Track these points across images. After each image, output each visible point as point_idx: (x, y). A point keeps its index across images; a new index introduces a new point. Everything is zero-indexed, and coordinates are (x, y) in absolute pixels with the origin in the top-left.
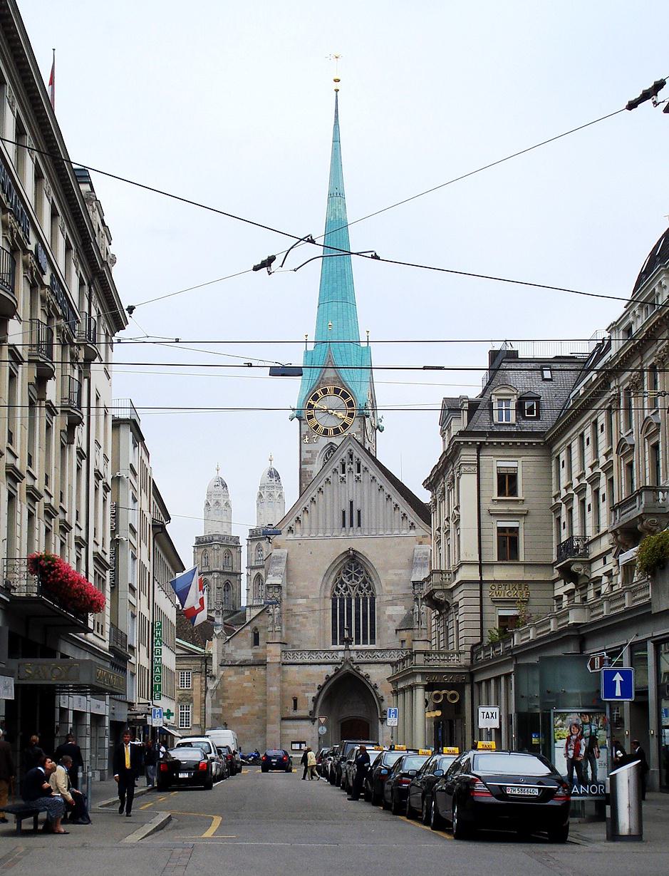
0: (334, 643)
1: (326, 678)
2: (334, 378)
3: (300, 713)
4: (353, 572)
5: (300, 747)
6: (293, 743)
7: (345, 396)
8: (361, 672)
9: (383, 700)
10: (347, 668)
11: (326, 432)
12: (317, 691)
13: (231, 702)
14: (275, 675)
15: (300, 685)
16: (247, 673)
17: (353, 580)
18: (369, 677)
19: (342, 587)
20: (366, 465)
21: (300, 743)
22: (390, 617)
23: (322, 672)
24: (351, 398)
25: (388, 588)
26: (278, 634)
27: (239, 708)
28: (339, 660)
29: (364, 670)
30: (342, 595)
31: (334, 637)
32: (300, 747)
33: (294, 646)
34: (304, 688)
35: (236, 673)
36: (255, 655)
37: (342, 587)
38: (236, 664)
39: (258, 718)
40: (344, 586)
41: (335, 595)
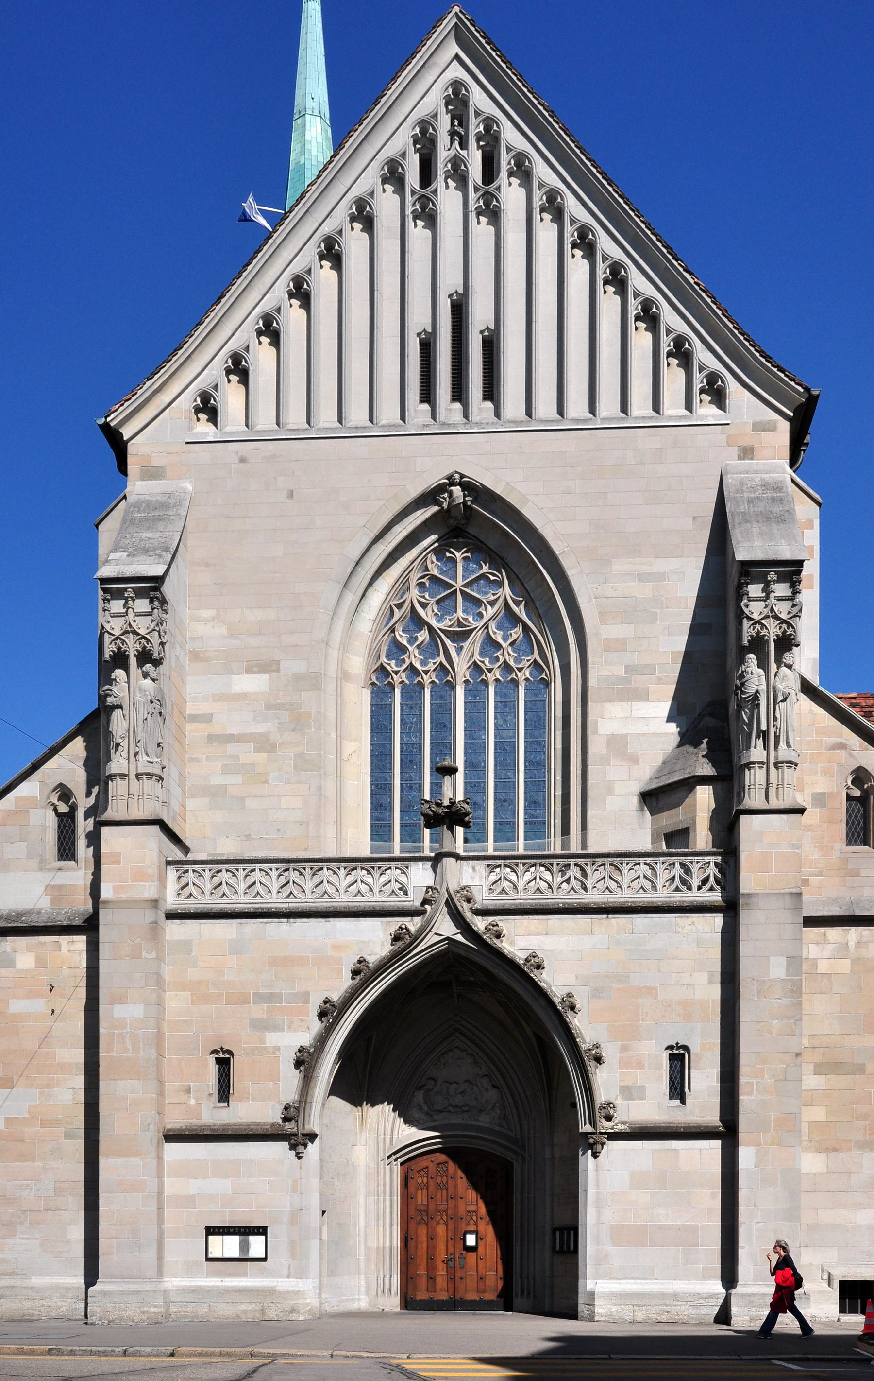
1: (355, 973)
4: (459, 583)
5: (244, 1247)
6: (211, 1231)
8: (506, 946)
12: (317, 1026)
14: (136, 955)
15: (243, 999)
17: (460, 613)
18: (539, 967)
19: (412, 640)
21: (245, 1231)
23: (337, 947)
28: (414, 900)
32: (244, 1247)
34: (259, 1011)
36: (56, 892)
41: (382, 671)
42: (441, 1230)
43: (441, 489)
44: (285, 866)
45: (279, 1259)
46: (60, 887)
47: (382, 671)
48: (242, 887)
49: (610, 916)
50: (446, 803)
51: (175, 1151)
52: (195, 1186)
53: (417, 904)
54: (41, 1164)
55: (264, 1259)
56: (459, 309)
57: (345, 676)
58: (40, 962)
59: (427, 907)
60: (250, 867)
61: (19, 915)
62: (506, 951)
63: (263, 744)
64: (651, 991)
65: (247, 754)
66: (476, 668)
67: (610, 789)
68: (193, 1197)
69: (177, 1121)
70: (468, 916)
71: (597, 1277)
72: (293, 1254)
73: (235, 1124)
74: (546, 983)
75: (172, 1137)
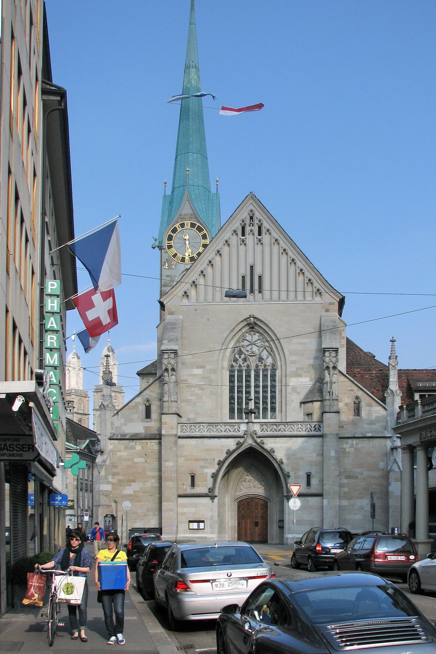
0: (232, 416)
2: (191, 214)
3: (198, 490)
5: (198, 526)
6: (190, 522)
7: (200, 229)
8: (265, 446)
9: (289, 476)
10: (250, 442)
11: (183, 260)
12: (217, 467)
13: (121, 477)
14: (171, 449)
15: (198, 460)
16: (138, 448)
18: (274, 452)
19: (240, 357)
20: (268, 227)
21: (199, 522)
22: (294, 389)
23: (222, 446)
24: (205, 232)
25: (293, 358)
26: (174, 404)
27: (130, 485)
28: (241, 433)
29: (269, 444)
30: (240, 366)
31: (232, 410)
32: (198, 526)
33: (189, 419)
34: (202, 463)
35: (126, 448)
36: (146, 428)
37: (240, 357)
38: (127, 437)
39: (150, 496)
40: (243, 356)
41: (232, 366)
42: (248, 521)
43: (248, 318)
44: (209, 424)
45: (208, 529)
46: (147, 427)
47: (232, 366)
48: (197, 430)
49: (292, 438)
50: (250, 409)
51: (181, 500)
52: (186, 510)
53: (242, 435)
54: (143, 503)
55: (204, 529)
56: (252, 267)
57: (223, 368)
58: (143, 448)
59: (245, 436)
60: (200, 425)
61: (137, 434)
62: (265, 448)
63: (201, 388)
64: (302, 458)
65: (197, 391)
66: (257, 366)
67: (292, 401)
68: (185, 513)
69: (181, 492)
70: (255, 438)
71: (288, 533)
72: (211, 528)
73: (196, 493)
74: (275, 456)
75: (180, 496)
